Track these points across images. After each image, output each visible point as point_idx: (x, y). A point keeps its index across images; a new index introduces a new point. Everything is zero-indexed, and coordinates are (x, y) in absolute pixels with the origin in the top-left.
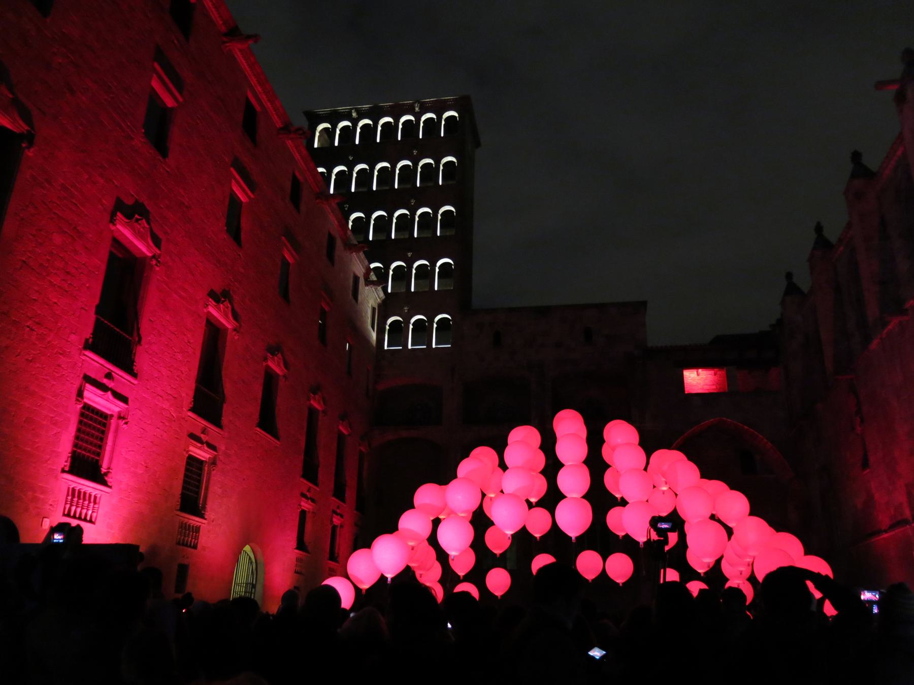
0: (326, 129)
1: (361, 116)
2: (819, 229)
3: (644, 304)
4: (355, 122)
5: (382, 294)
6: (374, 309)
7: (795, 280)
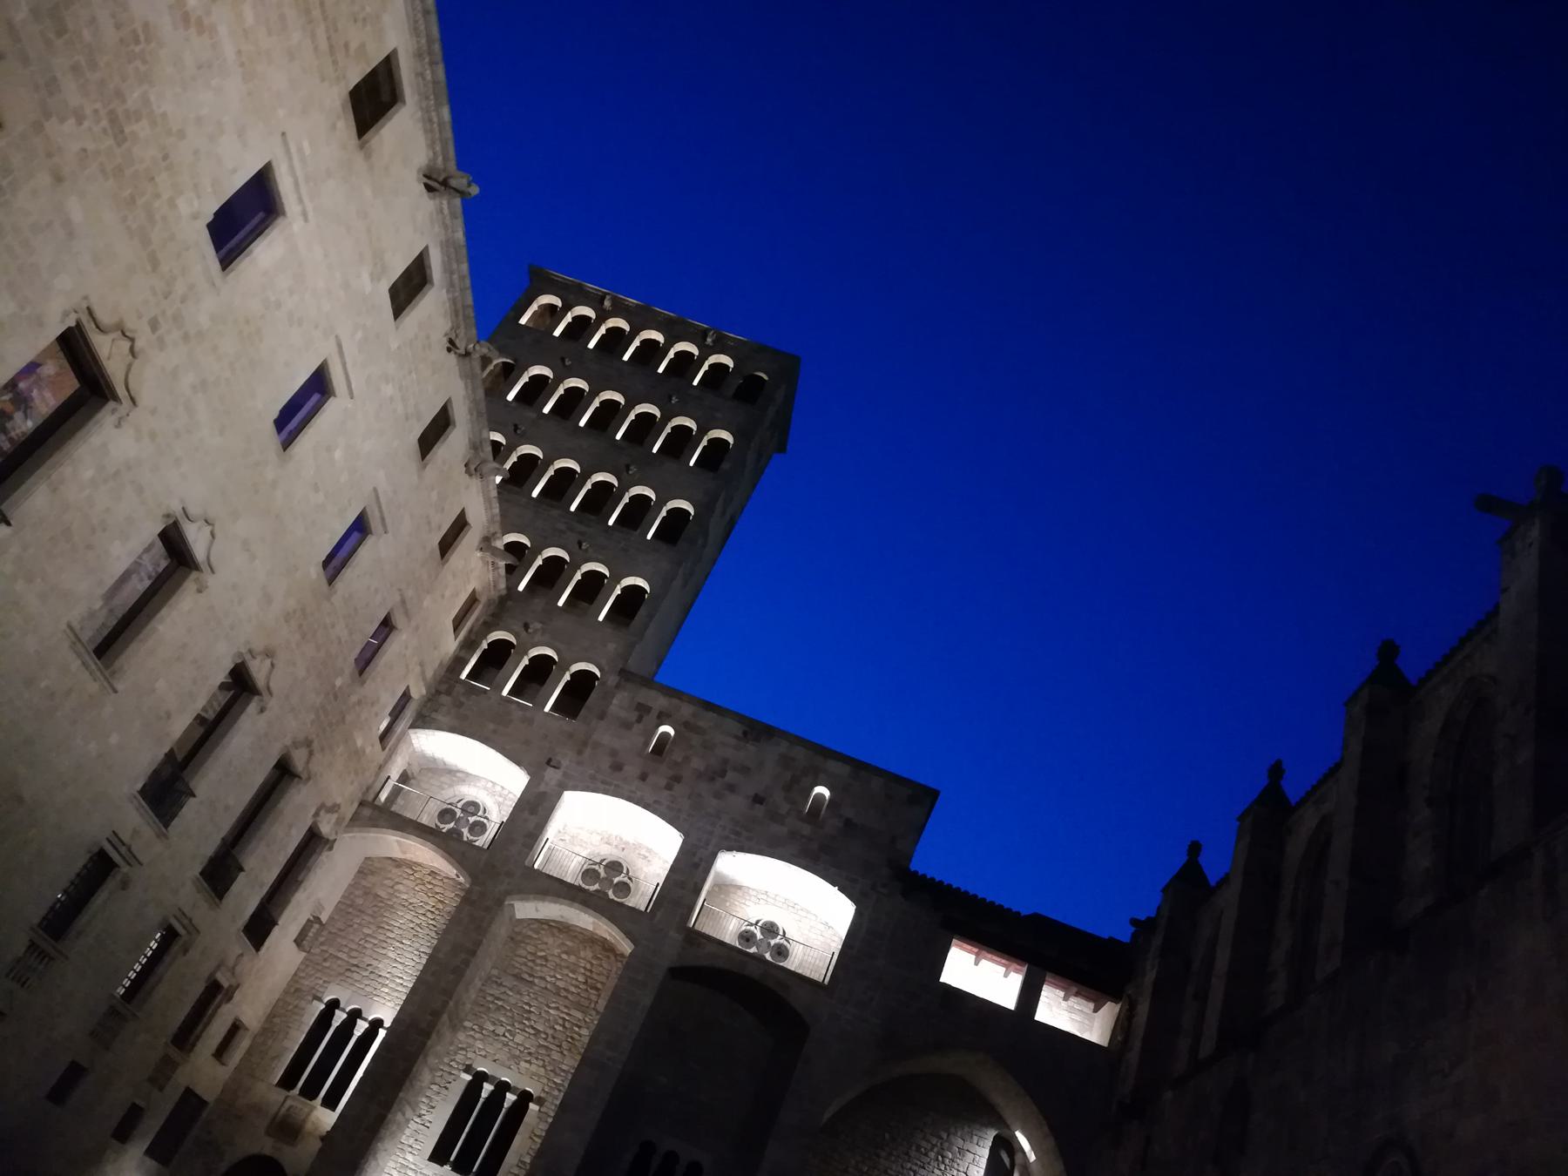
0: (552, 307)
1: (618, 310)
2: (1276, 771)
3: (934, 794)
4: (602, 318)
5: (502, 585)
6: (472, 600)
7: (1203, 860)
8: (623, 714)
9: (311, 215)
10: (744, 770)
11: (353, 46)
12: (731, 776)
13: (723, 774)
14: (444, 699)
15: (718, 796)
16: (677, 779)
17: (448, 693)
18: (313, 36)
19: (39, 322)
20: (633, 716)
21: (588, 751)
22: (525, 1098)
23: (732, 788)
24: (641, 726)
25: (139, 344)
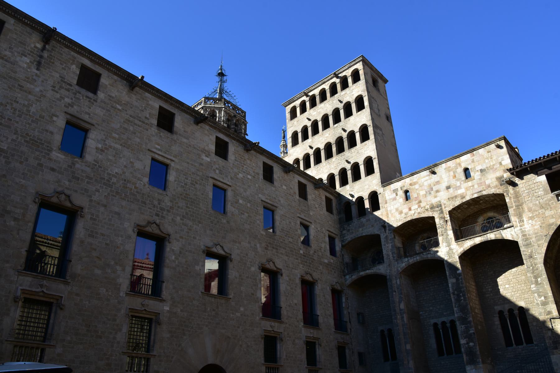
9: (174, 159)
10: (438, 183)
11: (148, 116)
12: (435, 189)
13: (432, 189)
14: (344, 232)
15: (436, 197)
16: (420, 202)
17: (344, 229)
18: (135, 124)
19: (129, 237)
20: (394, 195)
23: (437, 191)
24: (398, 196)
25: (158, 222)
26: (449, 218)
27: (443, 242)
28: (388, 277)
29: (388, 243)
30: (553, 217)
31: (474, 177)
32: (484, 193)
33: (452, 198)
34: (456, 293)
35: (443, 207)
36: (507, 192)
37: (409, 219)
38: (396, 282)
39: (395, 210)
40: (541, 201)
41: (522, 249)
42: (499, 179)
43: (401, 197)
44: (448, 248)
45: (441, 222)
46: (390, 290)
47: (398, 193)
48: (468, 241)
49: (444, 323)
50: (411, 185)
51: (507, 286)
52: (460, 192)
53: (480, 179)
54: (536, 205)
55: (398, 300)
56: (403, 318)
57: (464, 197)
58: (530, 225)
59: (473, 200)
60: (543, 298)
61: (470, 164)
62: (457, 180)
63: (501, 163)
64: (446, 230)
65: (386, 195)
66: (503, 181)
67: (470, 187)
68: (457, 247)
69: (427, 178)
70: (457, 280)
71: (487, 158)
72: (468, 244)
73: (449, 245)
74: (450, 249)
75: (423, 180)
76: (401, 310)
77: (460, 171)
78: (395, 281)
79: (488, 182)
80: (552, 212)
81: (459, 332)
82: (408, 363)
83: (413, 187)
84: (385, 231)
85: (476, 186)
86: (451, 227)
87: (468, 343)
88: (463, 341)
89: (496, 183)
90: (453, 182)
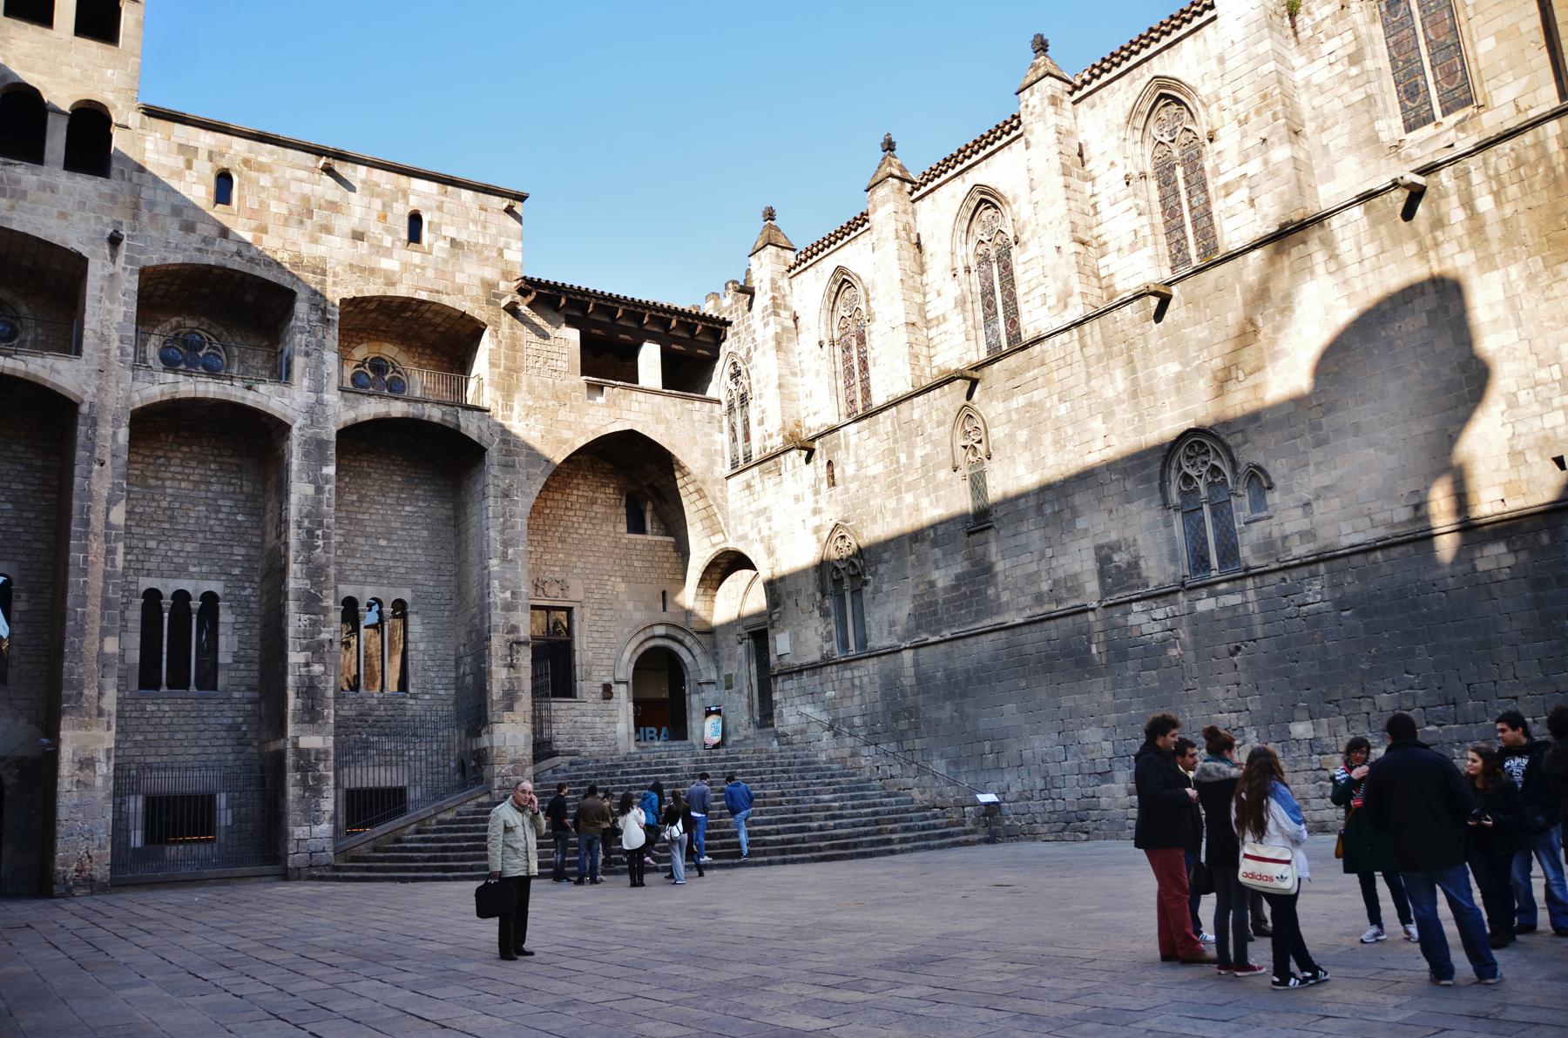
8: (164, 160)
10: (334, 206)
13: (310, 213)
15: (314, 241)
20: (180, 162)
21: (145, 216)
22: (210, 599)
23: (327, 229)
26: (337, 317)
27: (303, 375)
28: (84, 409)
29: (112, 300)
30: (569, 428)
31: (430, 246)
32: (446, 300)
33: (362, 270)
34: (306, 523)
35: (330, 280)
36: (497, 325)
37: (211, 260)
38: (115, 433)
39: (167, 210)
40: (558, 381)
41: (495, 470)
42: (489, 286)
43: (201, 180)
44: (313, 396)
45: (313, 317)
46: (81, 454)
47: (195, 163)
48: (372, 400)
49: (181, 597)
50: (246, 162)
51: (383, 543)
52: (386, 264)
53: (445, 261)
54: (545, 385)
55: (105, 493)
56: (111, 551)
57: (393, 284)
58: (523, 424)
59: (407, 303)
60: (508, 594)
61: (429, 209)
62: (389, 230)
63: (501, 252)
64: (321, 345)
65: (149, 145)
66: (496, 296)
67: (416, 266)
68: (341, 403)
69: (303, 174)
70: (319, 490)
71: (475, 222)
72: (371, 408)
73: (318, 389)
74: (320, 402)
75: (289, 173)
76: (108, 525)
77: (401, 212)
78: (110, 431)
79: (460, 278)
80: (572, 417)
81: (291, 631)
82: (101, 694)
83: (253, 174)
84: (113, 257)
85: (430, 273)
86: (336, 344)
87: (307, 665)
88: (295, 657)
89: (478, 291)
90: (374, 228)
